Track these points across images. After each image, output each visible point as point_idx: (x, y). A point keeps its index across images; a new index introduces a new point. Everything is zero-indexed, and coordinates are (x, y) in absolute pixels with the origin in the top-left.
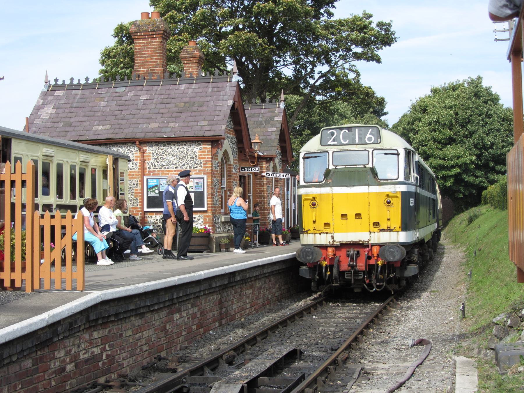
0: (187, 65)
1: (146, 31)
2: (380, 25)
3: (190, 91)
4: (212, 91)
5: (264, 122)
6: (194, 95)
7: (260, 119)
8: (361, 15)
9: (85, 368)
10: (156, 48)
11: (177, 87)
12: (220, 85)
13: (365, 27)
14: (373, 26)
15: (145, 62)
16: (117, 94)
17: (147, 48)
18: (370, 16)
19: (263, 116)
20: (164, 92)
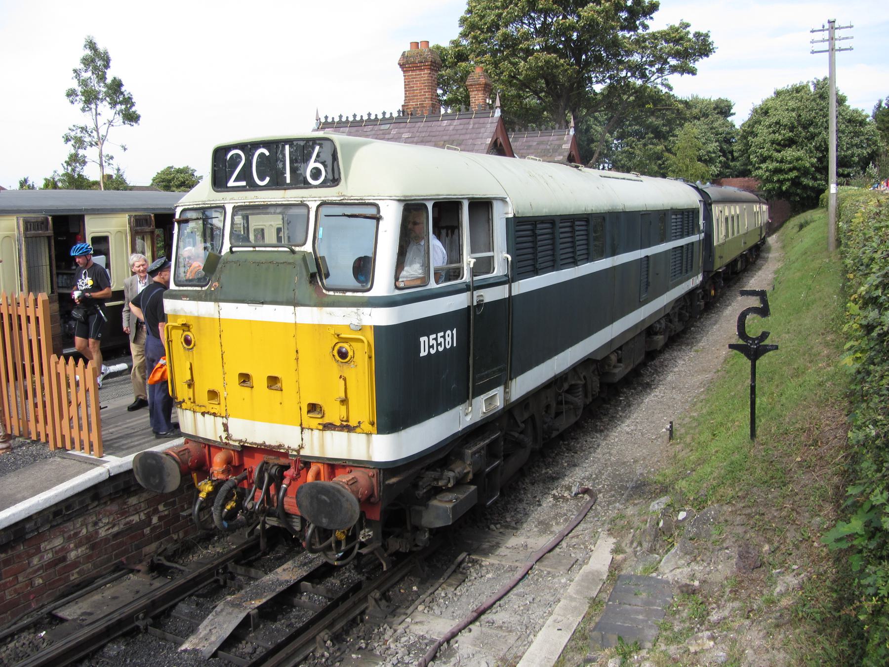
0: (474, 93)
1: (414, 63)
2: (698, 35)
3: (451, 128)
4: (473, 128)
6: (454, 132)
7: (548, 147)
8: (677, 25)
10: (424, 80)
11: (439, 123)
12: (482, 120)
13: (681, 38)
14: (691, 36)
16: (381, 132)
18: (688, 25)
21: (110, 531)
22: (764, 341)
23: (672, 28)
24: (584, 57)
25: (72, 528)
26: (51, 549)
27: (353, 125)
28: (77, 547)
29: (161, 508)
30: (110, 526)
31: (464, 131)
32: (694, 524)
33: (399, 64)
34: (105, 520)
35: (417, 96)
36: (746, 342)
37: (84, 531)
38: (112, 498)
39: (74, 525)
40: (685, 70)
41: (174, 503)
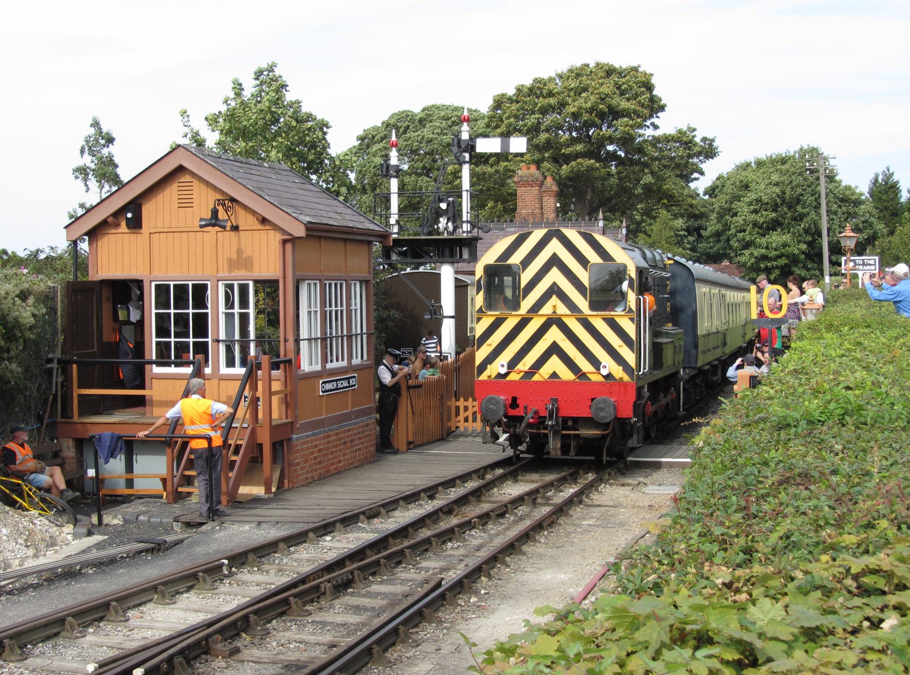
2: (704, 139)
8: (685, 129)
13: (691, 142)
18: (694, 130)
23: (680, 132)
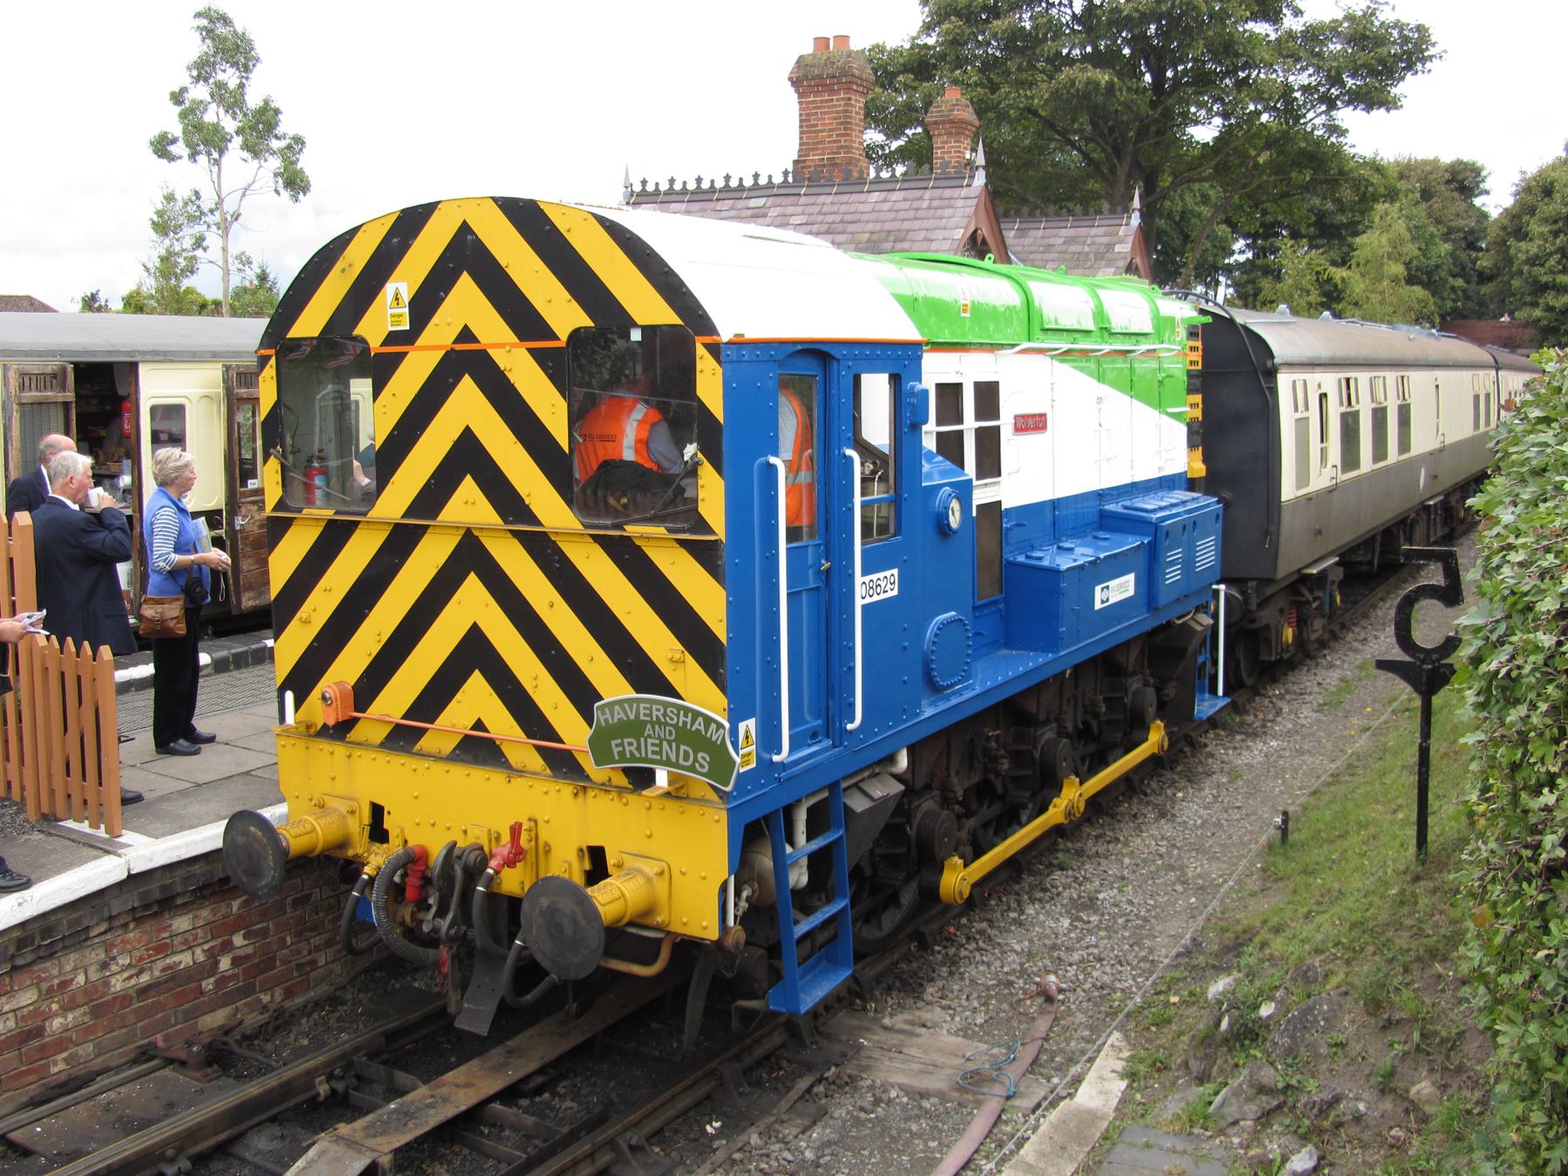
1: (820, 77)
3: (887, 206)
4: (929, 208)
5: (1092, 256)
6: (892, 215)
7: (1087, 249)
9: (135, 1011)
10: (838, 112)
11: (862, 197)
12: (947, 193)
15: (818, 143)
17: (822, 113)
19: (1094, 243)
20: (835, 208)
21: (133, 982)
22: (1448, 656)
23: (1350, 18)
24: (1169, 74)
25: (55, 972)
26: (14, 1011)
27: (695, 197)
28: (65, 1009)
29: (238, 940)
30: (134, 971)
31: (911, 214)
32: (1286, 1030)
33: (790, 79)
34: (124, 960)
35: (822, 142)
36: (1412, 656)
37: (81, 979)
38: (138, 916)
39: (61, 966)
40: (1373, 99)
41: (263, 933)
